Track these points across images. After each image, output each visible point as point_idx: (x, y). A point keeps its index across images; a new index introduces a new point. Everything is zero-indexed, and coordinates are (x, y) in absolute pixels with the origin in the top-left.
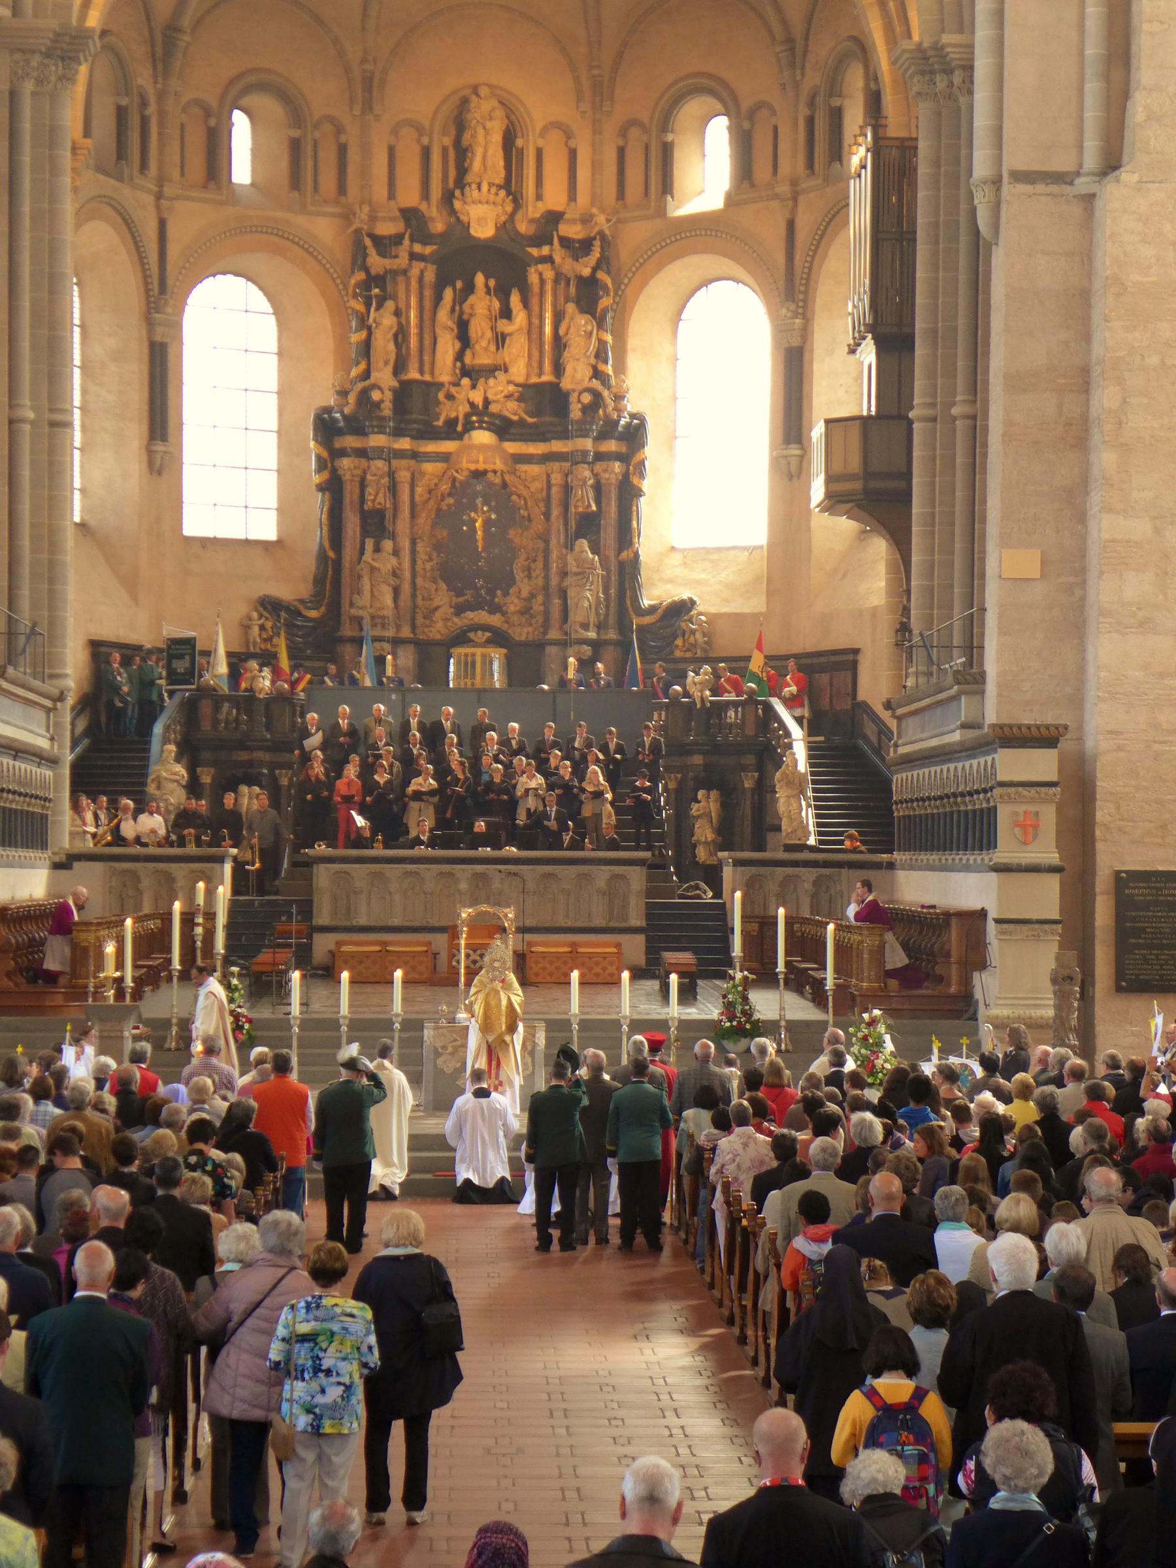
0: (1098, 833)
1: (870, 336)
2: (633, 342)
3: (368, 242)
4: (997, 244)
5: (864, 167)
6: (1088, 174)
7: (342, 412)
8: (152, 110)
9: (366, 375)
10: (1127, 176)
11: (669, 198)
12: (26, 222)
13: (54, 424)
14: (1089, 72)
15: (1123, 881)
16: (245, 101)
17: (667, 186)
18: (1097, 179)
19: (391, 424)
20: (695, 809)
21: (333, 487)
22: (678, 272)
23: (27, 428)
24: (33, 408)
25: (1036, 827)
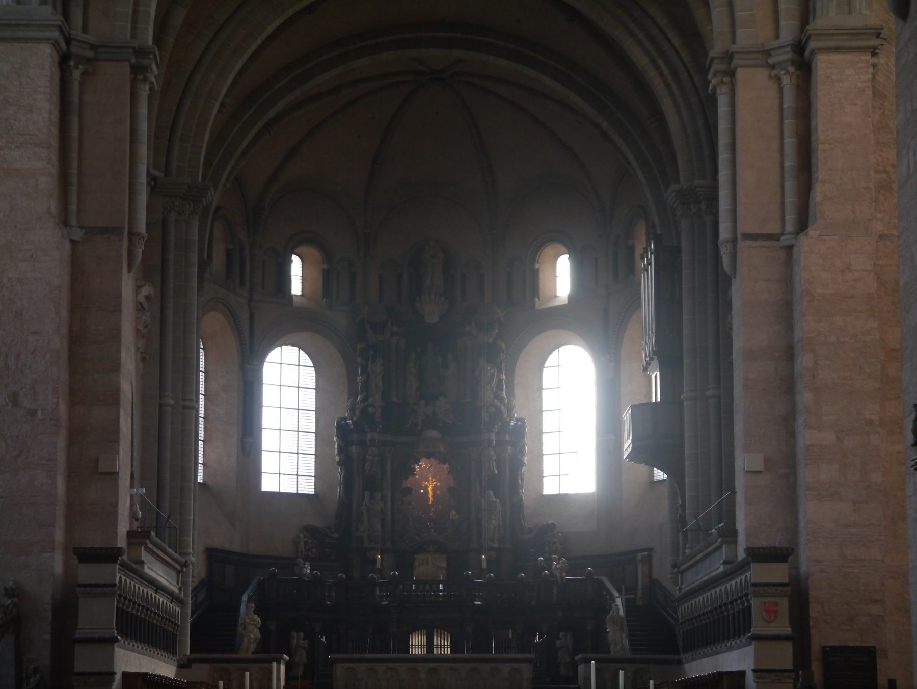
0: (811, 623)
2: (517, 380)
4: (735, 277)
6: (788, 234)
9: (365, 400)
10: (812, 232)
11: (537, 299)
13: (184, 407)
14: (787, 175)
15: (828, 652)
16: (298, 250)
18: (793, 236)
19: (380, 426)
20: (558, 643)
21: (346, 461)
22: (540, 340)
23: (169, 409)
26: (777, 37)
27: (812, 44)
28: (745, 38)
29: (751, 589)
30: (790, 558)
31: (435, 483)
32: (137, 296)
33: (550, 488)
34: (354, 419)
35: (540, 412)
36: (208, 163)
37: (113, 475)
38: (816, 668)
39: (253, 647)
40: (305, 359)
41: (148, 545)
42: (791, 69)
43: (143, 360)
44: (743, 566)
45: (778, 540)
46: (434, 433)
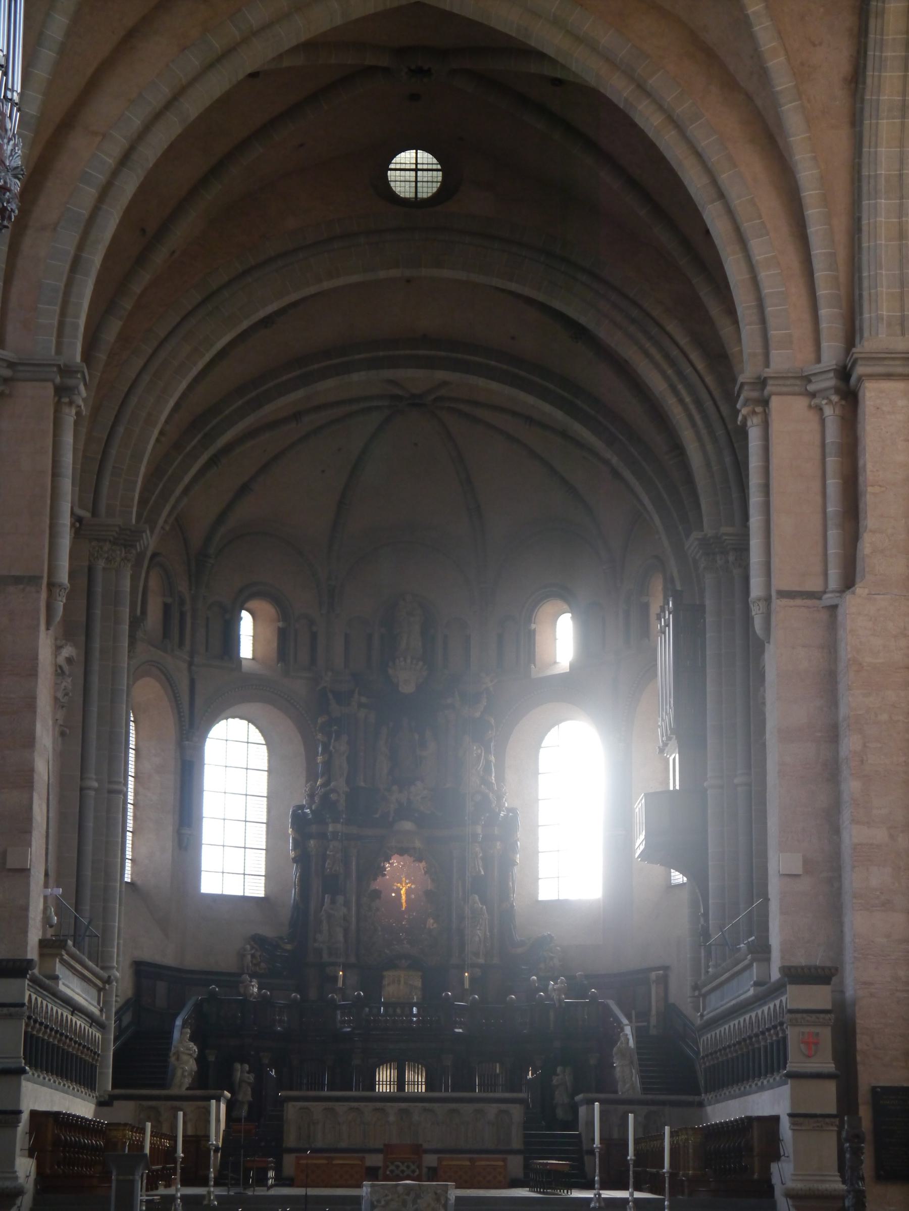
0: (859, 1058)
1: (674, 737)
3: (330, 696)
4: (769, 642)
5: (668, 625)
6: (832, 592)
7: (310, 808)
8: (188, 607)
9: (325, 784)
10: (860, 590)
11: (533, 666)
12: (97, 654)
13: (110, 792)
15: (878, 1094)
16: (249, 604)
17: (531, 656)
18: (838, 595)
19: (344, 816)
20: (555, 1080)
21: (302, 858)
23: (92, 793)
24: (97, 780)
25: (816, 1044)
26: (818, 360)
27: (860, 370)
28: (780, 361)
29: (787, 1017)
30: (834, 980)
31: (409, 885)
32: (56, 657)
33: (546, 892)
34: (313, 807)
35: (537, 800)
36: (143, 501)
37: (24, 872)
38: (865, 1113)
39: (187, 1081)
40: (256, 735)
41: (64, 957)
42: (835, 398)
43: (63, 734)
44: (778, 989)
45: (819, 958)
46: (408, 826)
